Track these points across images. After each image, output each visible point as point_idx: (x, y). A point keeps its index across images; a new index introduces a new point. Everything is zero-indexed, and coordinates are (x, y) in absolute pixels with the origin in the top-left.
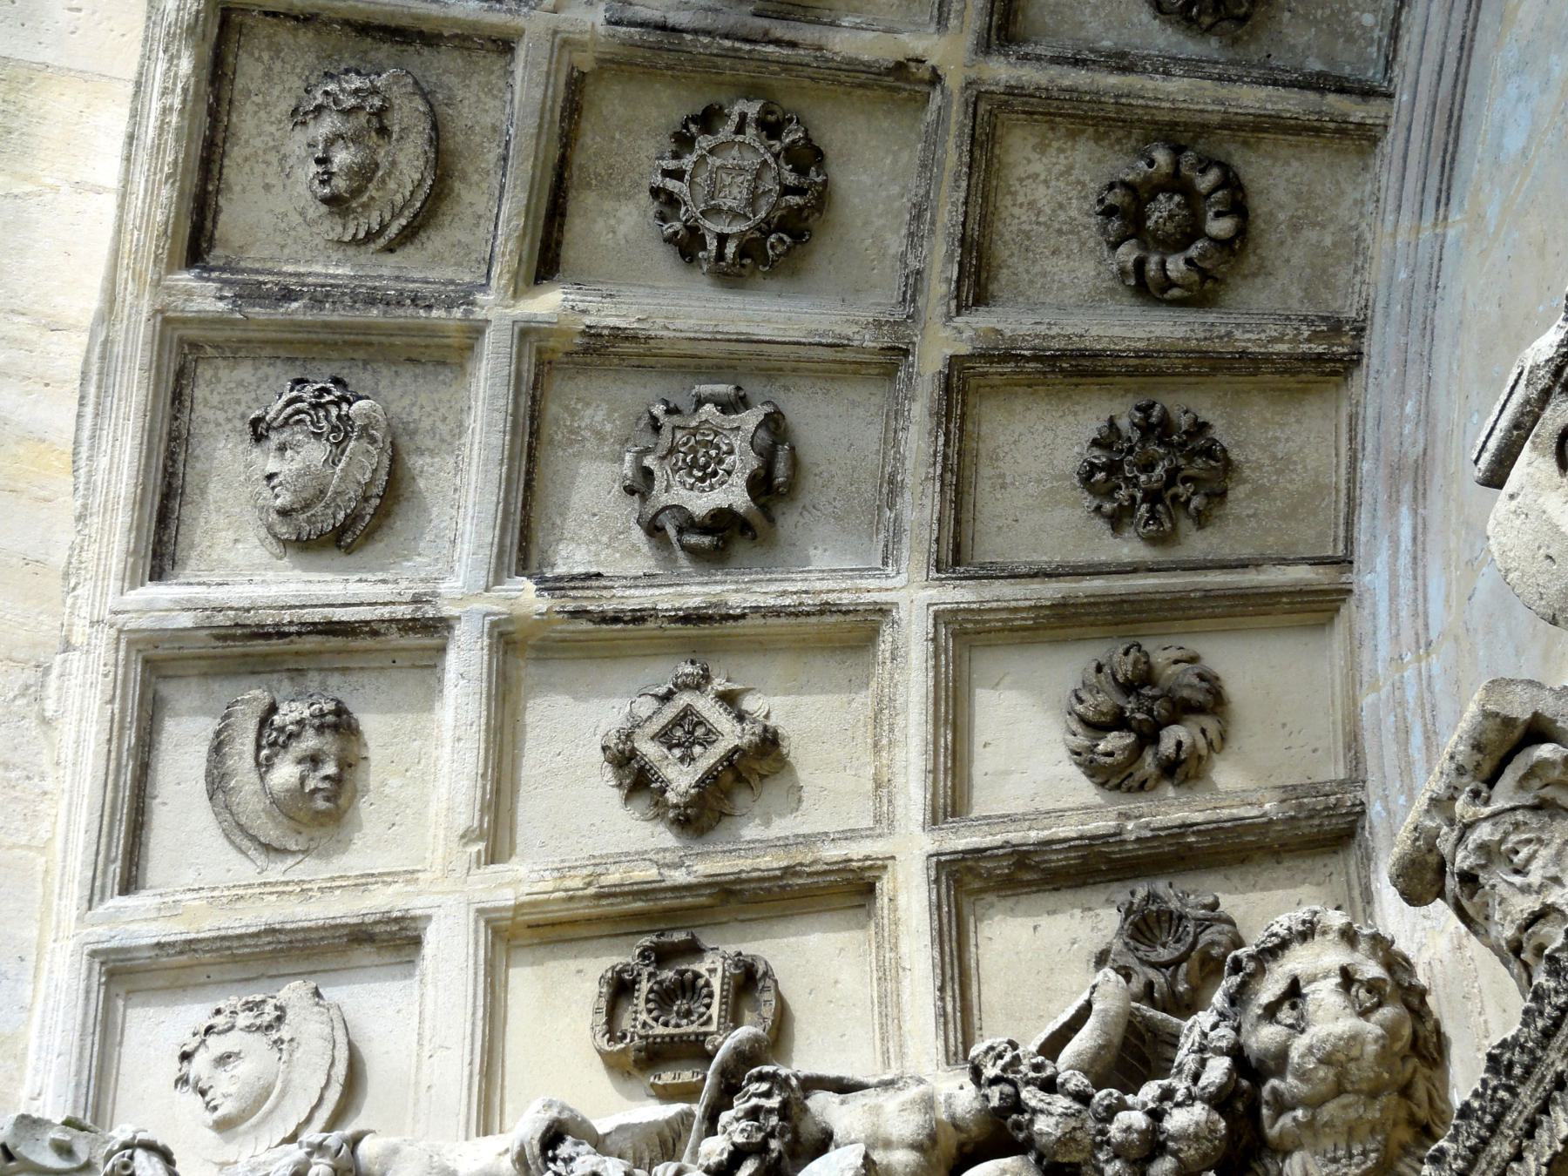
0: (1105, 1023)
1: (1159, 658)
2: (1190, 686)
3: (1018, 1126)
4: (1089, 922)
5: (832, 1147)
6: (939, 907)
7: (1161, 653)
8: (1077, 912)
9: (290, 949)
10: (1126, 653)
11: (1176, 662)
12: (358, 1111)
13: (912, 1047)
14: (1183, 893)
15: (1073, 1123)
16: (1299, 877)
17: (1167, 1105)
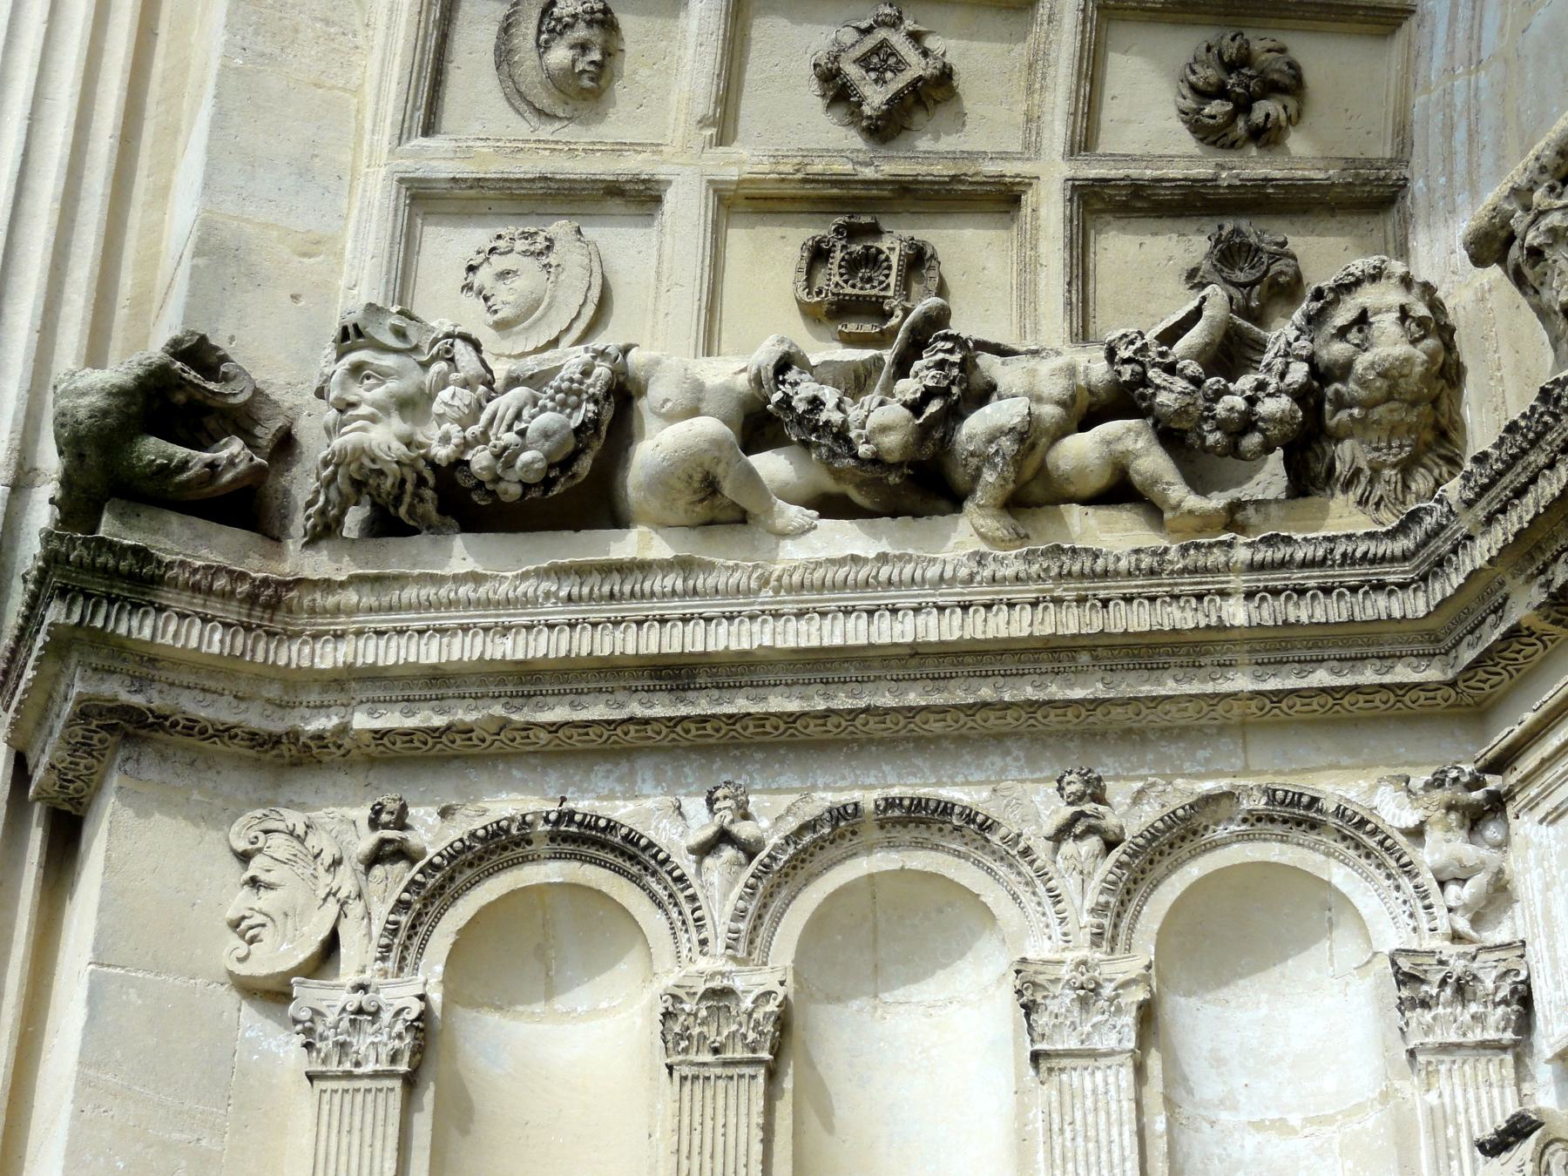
0: (1212, 327)
1: (1257, 47)
2: (1280, 71)
3: (1143, 397)
4: (1182, 246)
5: (995, 397)
6: (1071, 221)
7: (1259, 42)
8: (1175, 236)
10: (1233, 39)
11: (1269, 51)
12: (606, 326)
13: (1045, 326)
14: (1260, 231)
15: (1188, 400)
16: (1348, 229)
17: (1261, 394)
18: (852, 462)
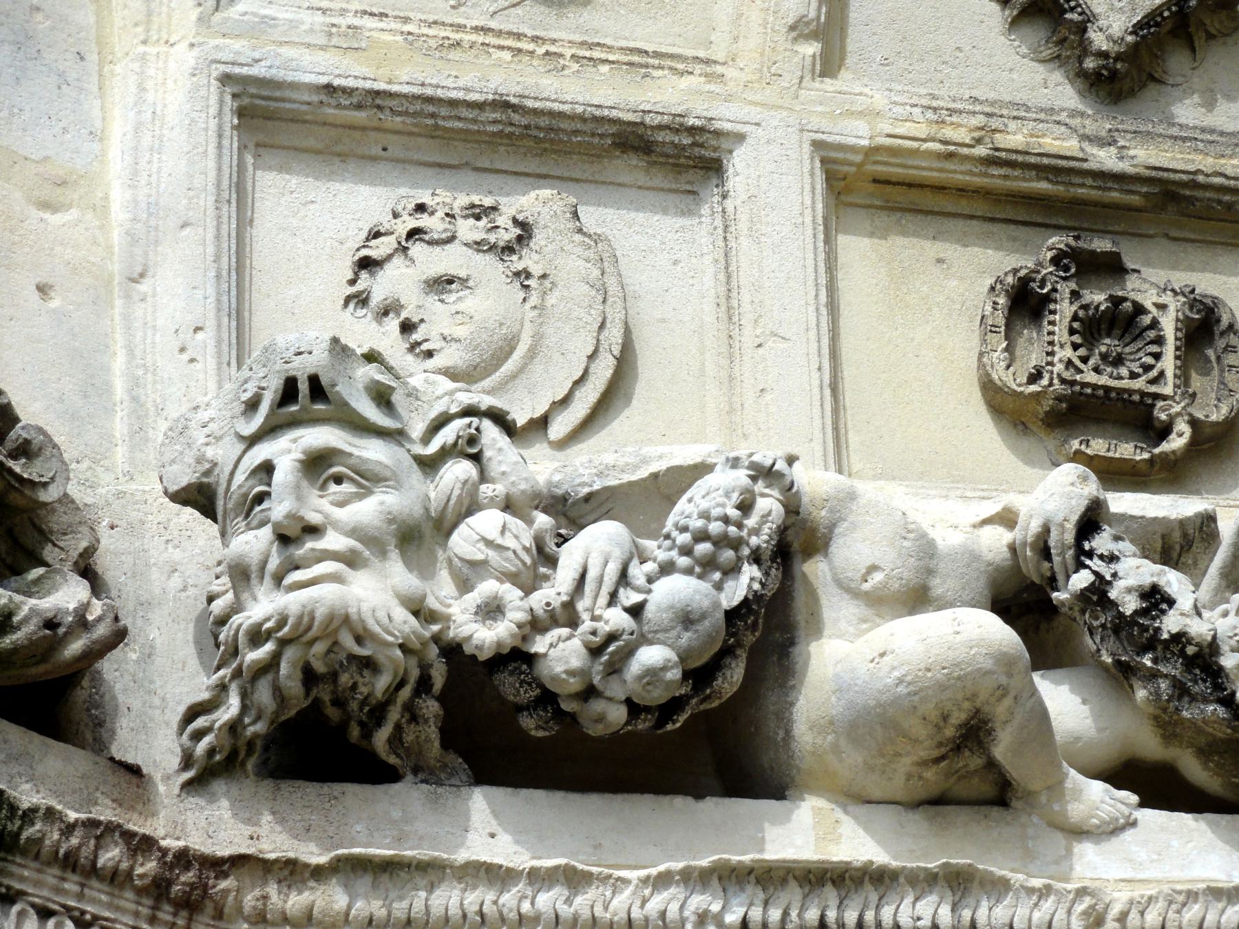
9: (522, 137)
12: (628, 401)
18: (1221, 711)
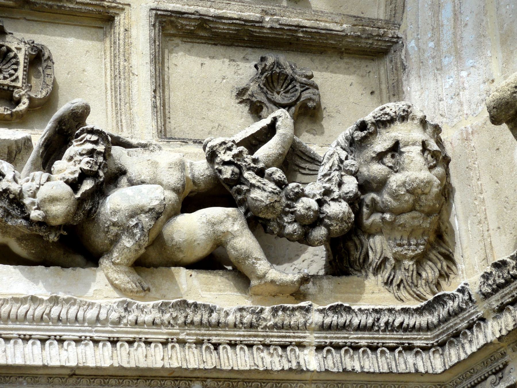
0: (284, 142)
3: (239, 192)
4: (233, 69)
5: (124, 180)
6: (155, 42)
8: (227, 61)
13: (138, 122)
14: (291, 63)
15: (276, 198)
16: (352, 69)
17: (327, 199)
18: (24, 222)
